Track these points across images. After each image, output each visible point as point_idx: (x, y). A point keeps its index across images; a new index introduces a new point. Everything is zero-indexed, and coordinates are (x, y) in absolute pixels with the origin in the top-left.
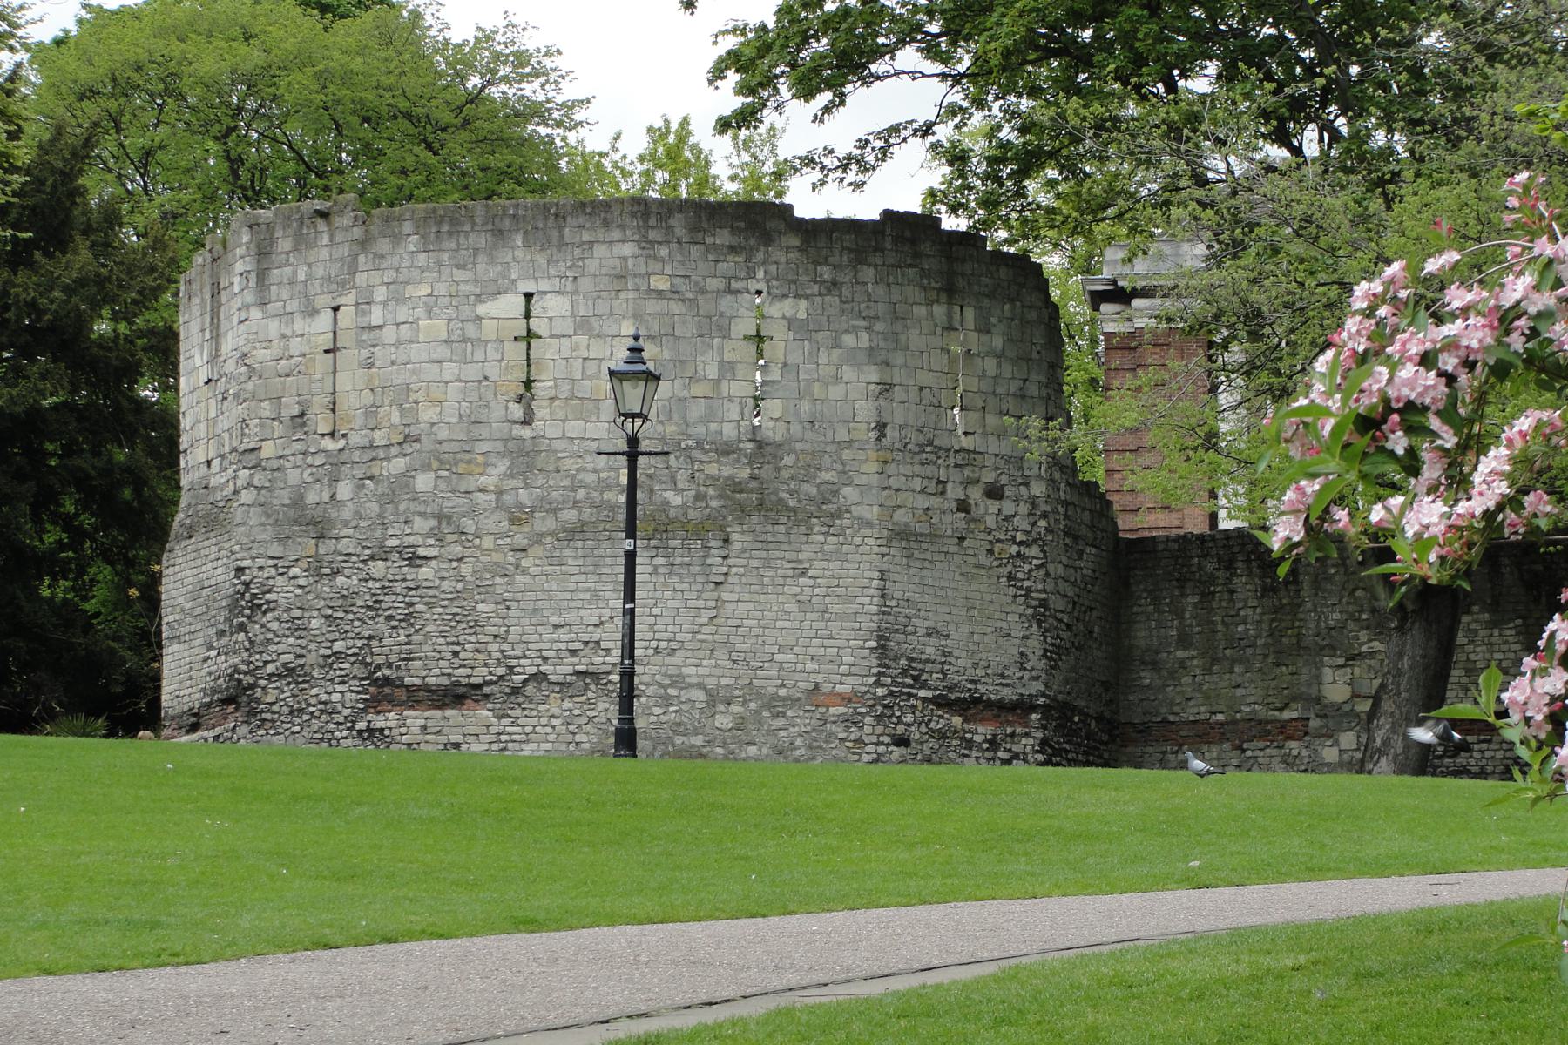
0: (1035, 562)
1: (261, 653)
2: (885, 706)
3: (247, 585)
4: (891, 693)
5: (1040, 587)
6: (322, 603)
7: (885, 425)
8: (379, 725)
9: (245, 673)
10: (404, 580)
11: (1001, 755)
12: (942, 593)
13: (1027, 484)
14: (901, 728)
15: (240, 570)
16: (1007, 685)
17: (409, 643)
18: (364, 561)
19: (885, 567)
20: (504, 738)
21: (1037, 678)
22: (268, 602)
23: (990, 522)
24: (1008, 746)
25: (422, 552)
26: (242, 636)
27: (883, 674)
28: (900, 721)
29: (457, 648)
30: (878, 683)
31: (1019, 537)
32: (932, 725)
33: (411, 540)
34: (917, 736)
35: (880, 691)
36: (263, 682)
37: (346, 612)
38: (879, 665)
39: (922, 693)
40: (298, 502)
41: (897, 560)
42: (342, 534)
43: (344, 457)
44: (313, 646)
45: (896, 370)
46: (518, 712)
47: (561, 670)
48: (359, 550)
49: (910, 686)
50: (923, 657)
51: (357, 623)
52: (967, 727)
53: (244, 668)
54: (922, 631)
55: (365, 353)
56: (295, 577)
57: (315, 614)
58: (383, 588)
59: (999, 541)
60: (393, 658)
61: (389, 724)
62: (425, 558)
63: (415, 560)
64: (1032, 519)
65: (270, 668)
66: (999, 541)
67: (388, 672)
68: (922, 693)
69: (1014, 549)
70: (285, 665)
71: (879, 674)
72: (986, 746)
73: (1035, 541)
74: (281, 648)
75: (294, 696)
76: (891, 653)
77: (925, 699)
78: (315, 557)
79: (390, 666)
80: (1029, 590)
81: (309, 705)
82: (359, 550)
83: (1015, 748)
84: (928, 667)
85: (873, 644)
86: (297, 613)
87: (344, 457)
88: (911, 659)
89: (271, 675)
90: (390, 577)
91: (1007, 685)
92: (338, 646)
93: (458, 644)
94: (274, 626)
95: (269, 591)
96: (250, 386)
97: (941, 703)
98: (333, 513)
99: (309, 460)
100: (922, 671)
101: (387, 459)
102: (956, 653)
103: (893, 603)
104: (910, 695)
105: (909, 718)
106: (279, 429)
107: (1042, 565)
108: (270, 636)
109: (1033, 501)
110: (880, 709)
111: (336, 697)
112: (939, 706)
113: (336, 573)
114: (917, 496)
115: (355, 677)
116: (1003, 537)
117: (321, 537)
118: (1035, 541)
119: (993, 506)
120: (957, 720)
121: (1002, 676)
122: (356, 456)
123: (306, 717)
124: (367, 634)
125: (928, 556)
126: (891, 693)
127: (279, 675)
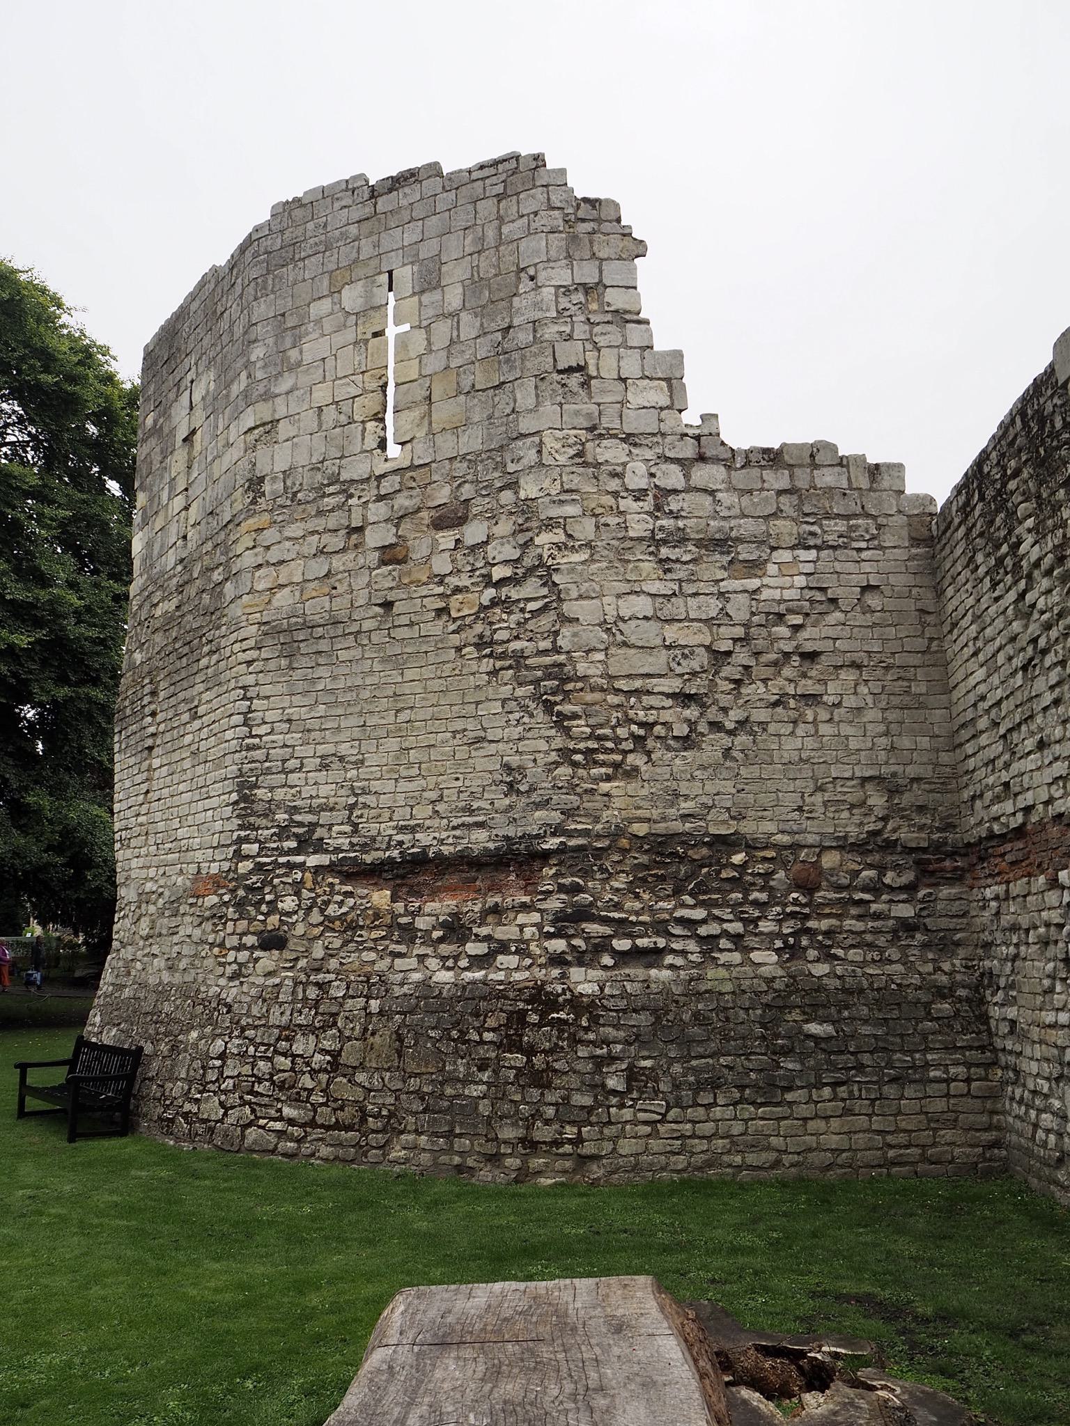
0: (532, 606)
2: (250, 889)
4: (259, 867)
5: (545, 645)
7: (261, 480)
11: (473, 948)
12: (349, 696)
13: (513, 486)
14: (274, 920)
16: (480, 825)
19: (251, 680)
21: (544, 804)
23: (442, 565)
24: (484, 931)
27: (246, 840)
28: (273, 908)
30: (239, 856)
31: (498, 573)
32: (332, 910)
34: (300, 929)
35: (245, 866)
38: (241, 827)
39: (313, 860)
41: (272, 665)
45: (278, 400)
49: (290, 852)
50: (316, 802)
52: (399, 907)
54: (312, 763)
59: (457, 590)
64: (522, 539)
66: (457, 590)
68: (313, 860)
69: (491, 592)
71: (240, 841)
72: (437, 934)
73: (530, 571)
76: (259, 807)
77: (318, 870)
80: (519, 657)
83: (501, 933)
84: (325, 817)
85: (234, 797)
88: (296, 810)
91: (480, 825)
97: (354, 872)
100: (313, 826)
102: (376, 786)
103: (264, 729)
104: (291, 866)
105: (288, 903)
107: (545, 608)
109: (526, 508)
110: (241, 893)
112: (347, 877)
114: (312, 562)
116: (464, 581)
118: (530, 571)
119: (446, 539)
120: (381, 898)
121: (471, 811)
125: (324, 645)
126: (259, 867)
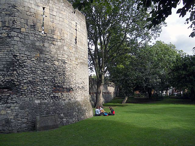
1: (22, 77)
3: (18, 60)
6: (41, 68)
8: (56, 95)
9: (16, 82)
10: (63, 66)
15: (15, 56)
17: (64, 79)
18: (53, 61)
20: (75, 98)
22: (24, 65)
25: (66, 61)
26: (15, 72)
29: (70, 81)
33: (64, 59)
36: (22, 84)
37: (48, 71)
40: (33, 44)
42: (47, 54)
43: (46, 38)
44: (38, 77)
46: (76, 93)
47: (80, 86)
48: (51, 58)
51: (50, 73)
53: (16, 80)
55: (51, 20)
56: (33, 61)
57: (39, 70)
58: (58, 67)
60: (60, 82)
61: (59, 95)
62: (66, 63)
63: (65, 63)
65: (25, 81)
67: (59, 85)
70: (29, 81)
74: (28, 76)
75: (32, 88)
78: (40, 57)
79: (59, 83)
81: (37, 90)
82: (51, 58)
86: (34, 69)
87: (46, 38)
89: (26, 83)
90: (59, 65)
92: (46, 78)
93: (70, 80)
94: (27, 71)
95: (25, 63)
96: (17, 14)
98: (44, 49)
99: (36, 36)
101: (57, 42)
106: (26, 27)
108: (25, 73)
111: (45, 89)
113: (44, 62)
115: (50, 85)
117: (41, 53)
122: (49, 39)
123: (35, 93)
124: (53, 76)
127: (27, 83)
